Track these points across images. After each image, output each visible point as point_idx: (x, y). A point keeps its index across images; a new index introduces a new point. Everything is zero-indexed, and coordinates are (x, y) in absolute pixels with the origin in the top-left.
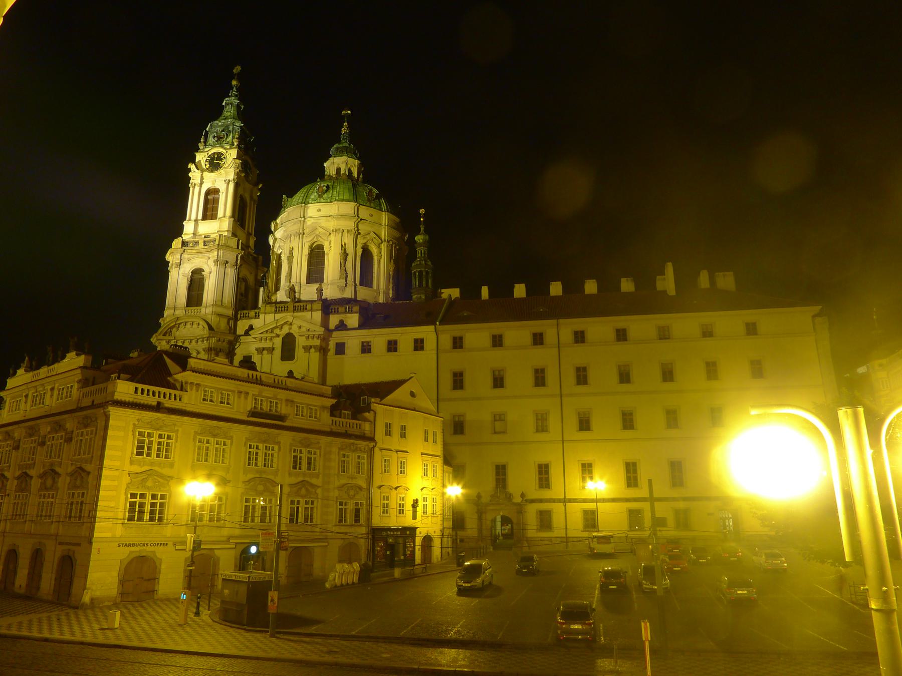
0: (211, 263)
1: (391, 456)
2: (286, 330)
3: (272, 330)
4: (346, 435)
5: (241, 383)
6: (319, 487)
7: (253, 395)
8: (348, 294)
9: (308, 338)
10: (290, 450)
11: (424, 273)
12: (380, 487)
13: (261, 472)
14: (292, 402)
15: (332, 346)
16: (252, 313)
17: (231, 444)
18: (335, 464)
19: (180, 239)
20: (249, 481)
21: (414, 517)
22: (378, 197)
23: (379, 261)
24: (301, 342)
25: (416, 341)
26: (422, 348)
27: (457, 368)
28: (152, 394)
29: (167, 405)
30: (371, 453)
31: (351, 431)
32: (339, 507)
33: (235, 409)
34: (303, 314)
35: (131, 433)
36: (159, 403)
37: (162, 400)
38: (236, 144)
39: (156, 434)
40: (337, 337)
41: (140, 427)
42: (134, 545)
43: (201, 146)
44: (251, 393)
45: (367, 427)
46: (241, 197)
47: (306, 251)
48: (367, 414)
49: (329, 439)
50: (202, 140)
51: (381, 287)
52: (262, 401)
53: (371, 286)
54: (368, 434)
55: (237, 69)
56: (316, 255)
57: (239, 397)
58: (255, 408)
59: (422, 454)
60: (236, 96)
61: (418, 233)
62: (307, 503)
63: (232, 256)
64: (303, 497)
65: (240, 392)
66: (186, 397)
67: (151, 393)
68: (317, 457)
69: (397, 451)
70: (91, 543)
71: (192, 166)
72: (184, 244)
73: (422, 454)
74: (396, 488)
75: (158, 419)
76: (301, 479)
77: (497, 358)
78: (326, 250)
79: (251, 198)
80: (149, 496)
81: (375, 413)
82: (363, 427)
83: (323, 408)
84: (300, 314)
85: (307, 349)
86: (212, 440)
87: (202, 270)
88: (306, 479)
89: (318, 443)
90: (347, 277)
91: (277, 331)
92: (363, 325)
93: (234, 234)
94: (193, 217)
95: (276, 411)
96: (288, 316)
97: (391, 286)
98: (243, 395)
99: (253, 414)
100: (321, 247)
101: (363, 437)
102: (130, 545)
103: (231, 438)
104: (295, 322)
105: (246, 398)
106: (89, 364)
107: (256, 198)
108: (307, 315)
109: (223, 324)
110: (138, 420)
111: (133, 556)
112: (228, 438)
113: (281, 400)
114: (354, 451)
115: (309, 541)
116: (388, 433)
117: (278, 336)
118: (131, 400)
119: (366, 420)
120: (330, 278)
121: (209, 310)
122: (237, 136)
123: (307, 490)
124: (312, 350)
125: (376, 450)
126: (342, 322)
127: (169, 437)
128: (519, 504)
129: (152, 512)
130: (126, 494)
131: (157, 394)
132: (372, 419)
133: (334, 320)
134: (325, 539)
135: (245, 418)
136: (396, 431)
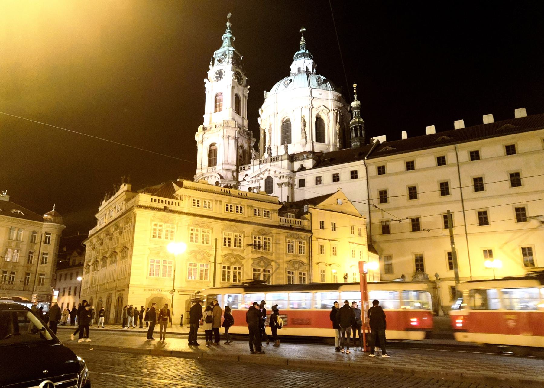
4: (291, 228)
5: (216, 195)
6: (272, 261)
7: (225, 202)
8: (308, 148)
10: (252, 238)
11: (358, 128)
12: (318, 264)
13: (233, 250)
14: (252, 207)
15: (297, 182)
16: (247, 167)
17: (212, 232)
18: (283, 247)
19: (201, 126)
20: (225, 256)
22: (325, 82)
24: (276, 181)
25: (352, 172)
26: (356, 177)
28: (161, 201)
29: (170, 209)
31: (294, 225)
32: (288, 275)
36: (165, 208)
37: (167, 205)
38: (230, 62)
40: (300, 175)
42: (153, 290)
43: (211, 67)
45: (305, 223)
46: (236, 95)
48: (306, 216)
49: (278, 230)
50: (211, 63)
53: (324, 142)
54: (307, 228)
55: (229, 15)
57: (216, 204)
59: (349, 243)
60: (230, 32)
61: (353, 100)
64: (262, 267)
65: (216, 201)
67: (160, 201)
69: (329, 240)
70: (128, 287)
71: (205, 80)
72: (204, 129)
73: (349, 243)
74: (330, 265)
76: (259, 255)
77: (411, 178)
79: (244, 95)
80: (162, 262)
81: (311, 214)
82: (303, 223)
83: (274, 210)
85: (280, 185)
86: (199, 229)
90: (306, 138)
91: (261, 176)
92: (315, 167)
93: (233, 119)
96: (267, 166)
97: (338, 140)
98: (218, 202)
100: (288, 121)
101: (303, 230)
102: (151, 290)
103: (212, 229)
104: (271, 168)
105: (221, 204)
106: (130, 189)
107: (247, 95)
108: (279, 163)
109: (229, 175)
111: (153, 296)
112: (210, 228)
114: (296, 239)
116: (322, 227)
117: (262, 179)
118: (148, 205)
122: (230, 57)
123: (264, 262)
124: (283, 186)
125: (313, 238)
126: (302, 165)
128: (434, 282)
129: (165, 271)
131: (164, 202)
132: (309, 218)
133: (297, 165)
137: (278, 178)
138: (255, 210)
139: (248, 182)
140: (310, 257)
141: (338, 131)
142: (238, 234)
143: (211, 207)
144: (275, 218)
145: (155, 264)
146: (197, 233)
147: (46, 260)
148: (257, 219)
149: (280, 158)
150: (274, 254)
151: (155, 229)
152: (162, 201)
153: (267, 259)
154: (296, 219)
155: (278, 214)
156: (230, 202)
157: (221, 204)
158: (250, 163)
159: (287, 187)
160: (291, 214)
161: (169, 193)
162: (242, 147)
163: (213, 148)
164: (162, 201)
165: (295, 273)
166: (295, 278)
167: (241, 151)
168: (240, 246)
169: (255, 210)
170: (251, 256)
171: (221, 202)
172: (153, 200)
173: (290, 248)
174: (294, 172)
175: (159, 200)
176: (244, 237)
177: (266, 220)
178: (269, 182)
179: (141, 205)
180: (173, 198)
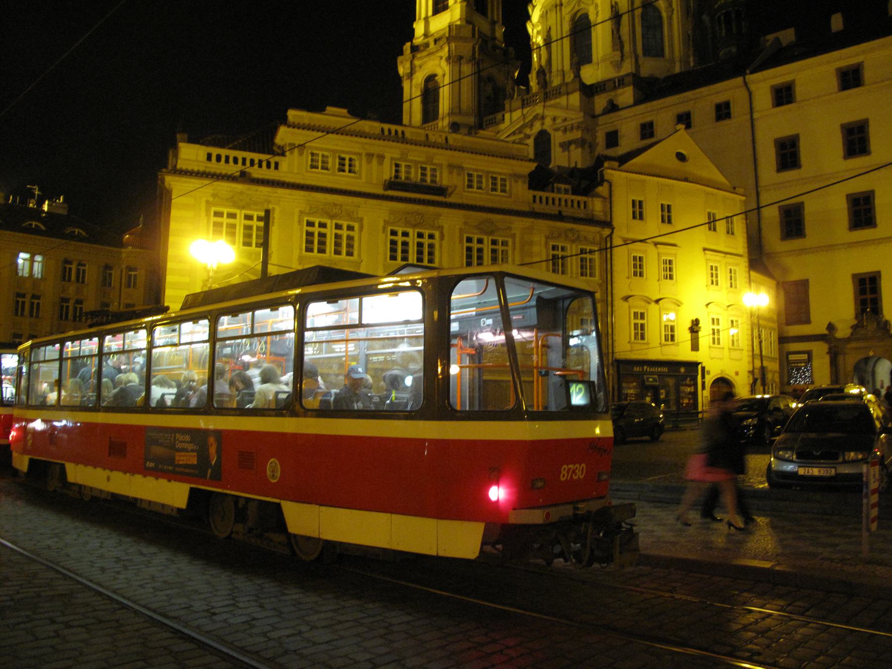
0: (444, 63)
1: (645, 252)
2: (537, 127)
3: (520, 130)
5: (367, 140)
7: (392, 159)
8: (628, 67)
9: (565, 131)
10: (461, 241)
11: (733, 16)
12: (626, 299)
14: (460, 168)
16: (499, 116)
19: (408, 44)
21: (695, 347)
23: (670, 18)
24: (557, 138)
26: (728, 116)
27: (786, 131)
30: (607, 248)
31: (567, 211)
33: (364, 180)
34: (558, 100)
36: (243, 174)
39: (241, 214)
41: (215, 205)
44: (388, 156)
45: (597, 206)
47: (566, 28)
49: (527, 222)
51: (677, 54)
53: (662, 55)
56: (581, 29)
57: (369, 162)
58: (396, 177)
59: (705, 249)
63: (466, 49)
65: (370, 156)
67: (231, 160)
72: (415, 49)
73: (705, 249)
74: (657, 301)
75: (241, 193)
78: (592, 17)
82: (590, 205)
83: (516, 176)
84: (553, 102)
85: (565, 146)
87: (435, 75)
89: (510, 228)
91: (527, 131)
92: (638, 102)
93: (468, 22)
94: (423, 16)
95: (432, 181)
97: (691, 52)
98: (375, 161)
99: (391, 185)
100: (586, 16)
101: (591, 221)
103: (361, 220)
104: (546, 113)
108: (563, 100)
110: (214, 196)
113: (441, 165)
114: (573, 242)
117: (528, 137)
118: (202, 169)
120: (601, 54)
121: (446, 122)
124: (573, 147)
131: (240, 161)
133: (600, 102)
135: (380, 191)
136: (652, 212)
137: (560, 133)
141: (690, 32)
142: (426, 233)
143: (357, 169)
144: (522, 194)
146: (323, 230)
148: (474, 197)
149: (563, 90)
154: (573, 197)
155: (526, 186)
156: (404, 157)
158: (504, 109)
159: (579, 150)
160: (563, 186)
161: (264, 142)
162: (490, 79)
163: (431, 85)
164: (236, 160)
167: (489, 89)
169: (470, 175)
172: (214, 158)
174: (594, 117)
176: (442, 237)
177: (496, 199)
178: (543, 141)
179: (184, 168)
180: (271, 152)
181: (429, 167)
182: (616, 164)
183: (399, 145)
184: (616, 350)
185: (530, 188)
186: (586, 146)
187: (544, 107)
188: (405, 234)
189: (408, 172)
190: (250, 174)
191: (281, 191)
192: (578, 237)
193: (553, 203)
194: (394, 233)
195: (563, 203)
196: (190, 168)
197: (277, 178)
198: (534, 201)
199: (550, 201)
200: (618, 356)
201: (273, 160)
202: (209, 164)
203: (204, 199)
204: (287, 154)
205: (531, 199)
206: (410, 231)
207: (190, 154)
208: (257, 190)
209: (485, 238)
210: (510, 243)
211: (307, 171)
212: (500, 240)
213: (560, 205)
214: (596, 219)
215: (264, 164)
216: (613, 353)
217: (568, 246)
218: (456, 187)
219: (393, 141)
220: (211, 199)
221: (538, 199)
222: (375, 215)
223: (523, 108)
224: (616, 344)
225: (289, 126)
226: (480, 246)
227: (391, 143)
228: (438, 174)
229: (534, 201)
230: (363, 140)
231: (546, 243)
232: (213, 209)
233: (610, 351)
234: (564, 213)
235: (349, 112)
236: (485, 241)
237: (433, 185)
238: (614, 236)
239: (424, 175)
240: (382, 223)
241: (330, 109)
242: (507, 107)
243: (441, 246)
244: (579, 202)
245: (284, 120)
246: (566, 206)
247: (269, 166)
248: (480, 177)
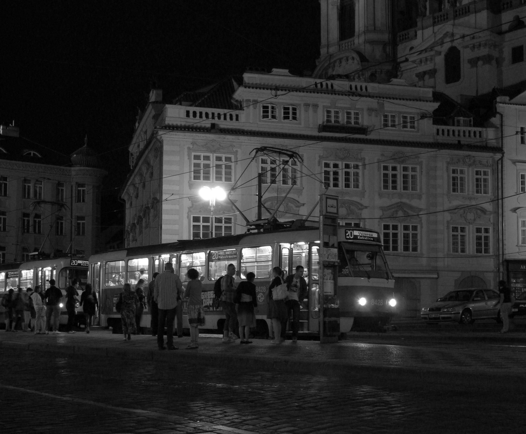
2: (447, 46)
3: (431, 48)
4: (459, 146)
7: (324, 107)
12: (515, 210)
15: (507, 53)
16: (411, 32)
18: (443, 181)
24: (466, 55)
29: (222, 126)
30: (498, 169)
31: (464, 140)
34: (466, 18)
35: (186, 158)
36: (213, 126)
37: (216, 121)
39: (213, 156)
41: (195, 151)
52: (337, 113)
54: (493, 143)
57: (306, 111)
58: (328, 121)
62: (406, 228)
65: (307, 105)
66: (243, 115)
67: (204, 115)
68: (418, 174)
75: (213, 141)
81: (502, 116)
84: (461, 20)
85: (473, 62)
88: (404, 200)
91: (438, 48)
95: (356, 123)
96: (447, 27)
99: (324, 128)
101: (485, 148)
104: (456, 31)
105: (315, 111)
106: (160, 99)
108: (470, 19)
109: (378, 53)
110: (193, 143)
113: (363, 109)
114: (470, 165)
115: (414, 272)
117: (440, 53)
118: (183, 124)
119: (493, 126)
121: (362, 39)
124: (480, 63)
125: (507, 163)
127: (228, 159)
130: (188, 217)
134: (436, 270)
135: (316, 133)
138: (386, 116)
139: (414, 62)
140: (498, 199)
144: (427, 129)
145: (201, 224)
147: (83, 228)
148: (389, 134)
150: (424, 197)
151: (196, 165)
152: (195, 114)
153: (411, 208)
157: (315, 111)
158: (416, 26)
159: (487, 66)
161: (224, 99)
164: (207, 115)
165: (467, 230)
166: (467, 238)
168: (357, 186)
169: (386, 116)
170: (379, 202)
171: (316, 106)
172: (191, 114)
173: (456, 184)
174: (501, 33)
175: (201, 113)
176: (364, 165)
177: (408, 135)
178: (453, 59)
179: (171, 123)
180: (231, 106)
181: (352, 112)
182: (507, 98)
183: (330, 95)
184: (506, 252)
185: (435, 123)
186: (494, 62)
187: (454, 25)
188: (336, 166)
189: (337, 117)
190: (218, 125)
191: (242, 138)
192: (474, 161)
193: (454, 135)
194: (327, 165)
195: (462, 134)
196: (175, 123)
197: (238, 127)
198: (438, 134)
199: (451, 133)
200: (507, 257)
201: (234, 113)
202: (188, 120)
203: (186, 147)
204: (245, 108)
205: (435, 131)
206: (340, 163)
207: (175, 113)
208: (224, 138)
209: (398, 166)
210: (418, 169)
211: (260, 121)
212: (410, 166)
213: (459, 135)
214: (489, 145)
215: (228, 117)
216: (503, 254)
217: (465, 169)
218: (374, 126)
219: (325, 93)
220: (191, 146)
221: (440, 132)
222: (312, 153)
223: (434, 26)
224: (505, 247)
225: (245, 87)
226: (394, 172)
227: (323, 95)
228: (360, 116)
229: (438, 134)
230: (302, 94)
231: (447, 168)
232: (193, 154)
233: (501, 253)
234: (462, 143)
235: (290, 72)
236: (398, 169)
237: (357, 126)
238: (505, 159)
239: (349, 118)
240: (317, 159)
241: (275, 70)
242: (419, 24)
243: (363, 174)
244: (475, 132)
245: (241, 82)
246: (464, 136)
247: (231, 119)
248: (393, 117)
